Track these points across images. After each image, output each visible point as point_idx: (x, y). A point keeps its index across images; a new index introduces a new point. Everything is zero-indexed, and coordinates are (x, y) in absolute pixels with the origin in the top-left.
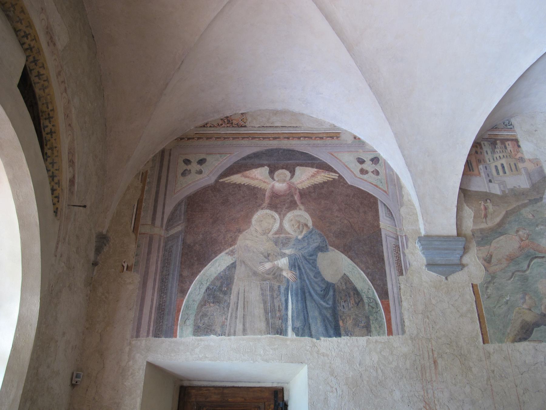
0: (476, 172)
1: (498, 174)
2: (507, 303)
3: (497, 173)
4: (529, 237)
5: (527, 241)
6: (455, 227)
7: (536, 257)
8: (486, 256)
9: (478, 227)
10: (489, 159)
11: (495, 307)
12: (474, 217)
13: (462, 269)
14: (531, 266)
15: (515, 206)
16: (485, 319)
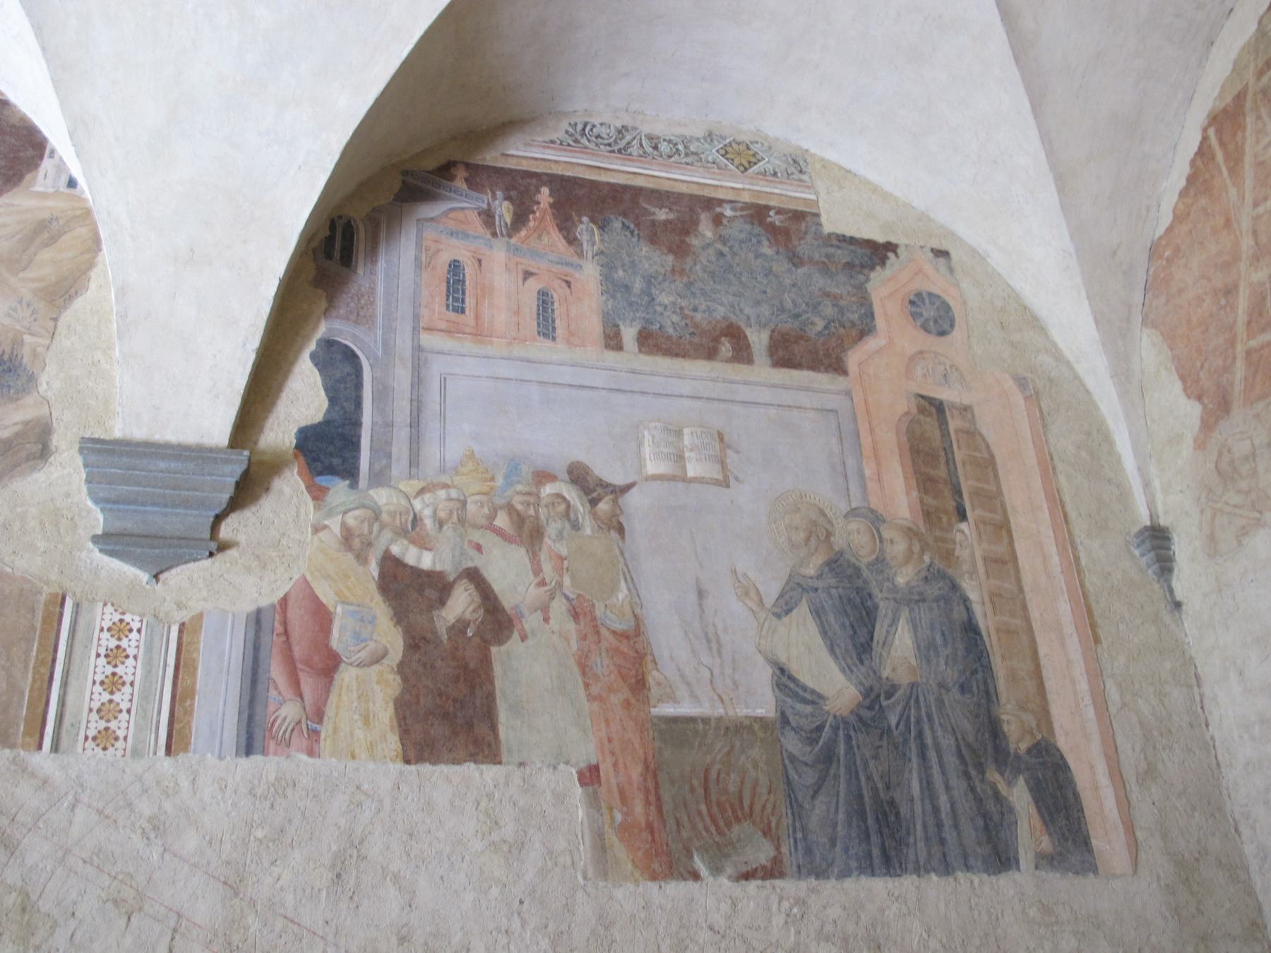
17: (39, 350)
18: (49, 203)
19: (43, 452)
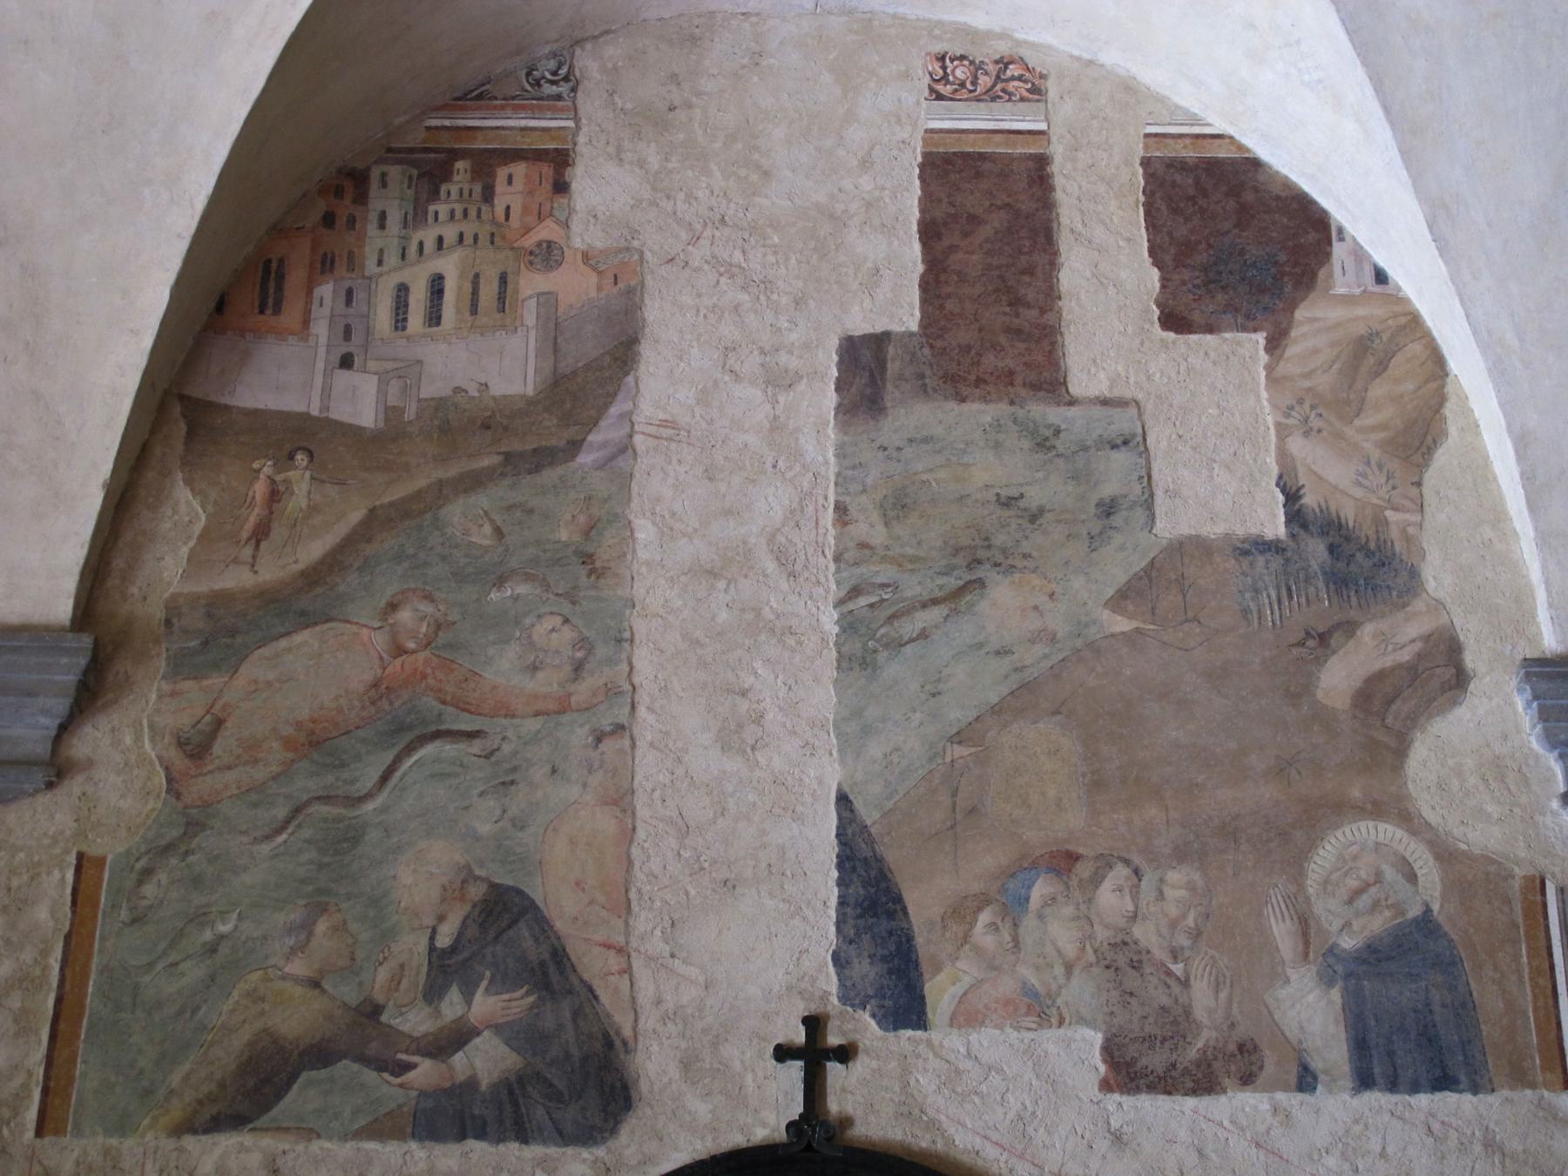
0: (290, 316)
1: (396, 328)
2: (212, 949)
3: (397, 321)
4: (441, 634)
5: (422, 656)
6: (70, 584)
7: (437, 735)
8: (194, 727)
9: (203, 586)
10: (381, 251)
11: (151, 965)
12: (202, 537)
13: (50, 785)
14: (398, 774)
15: (421, 483)
16: (85, 1022)
17: (1411, 530)
18: (1360, 311)
19: (1459, 680)
